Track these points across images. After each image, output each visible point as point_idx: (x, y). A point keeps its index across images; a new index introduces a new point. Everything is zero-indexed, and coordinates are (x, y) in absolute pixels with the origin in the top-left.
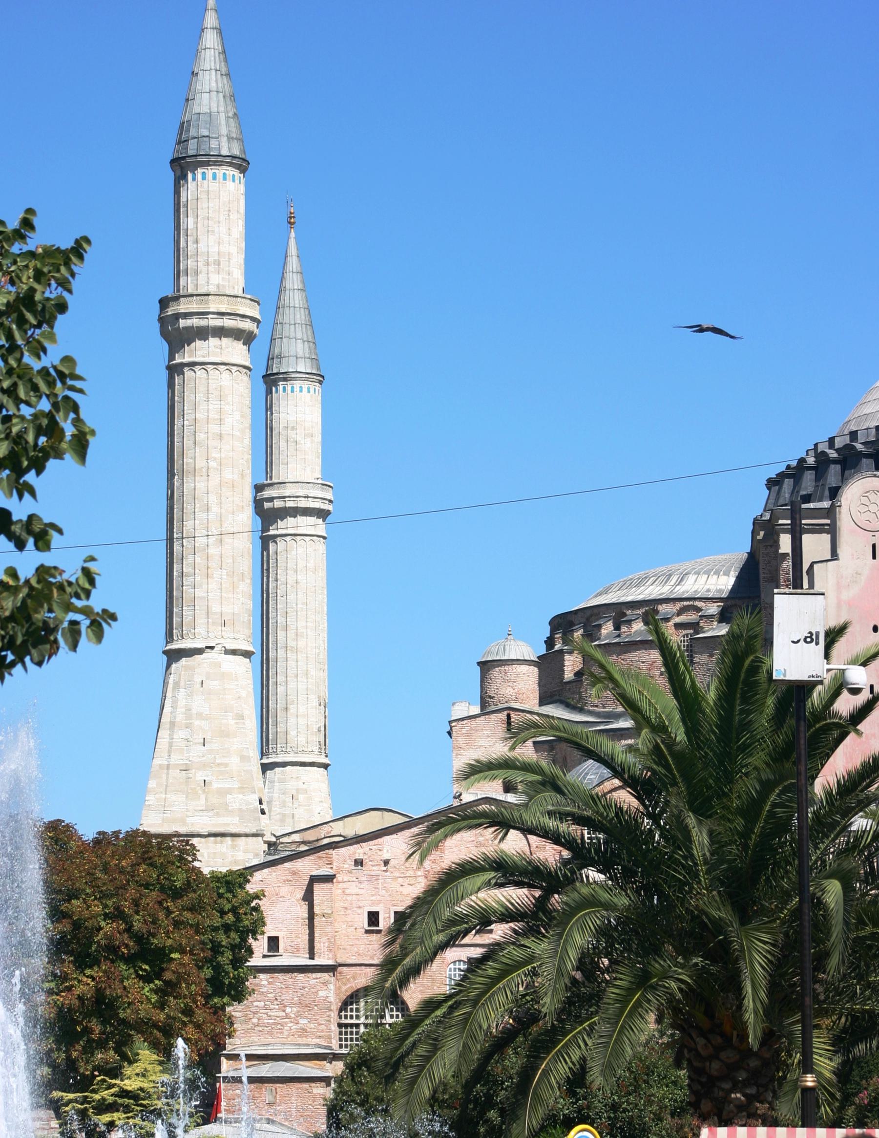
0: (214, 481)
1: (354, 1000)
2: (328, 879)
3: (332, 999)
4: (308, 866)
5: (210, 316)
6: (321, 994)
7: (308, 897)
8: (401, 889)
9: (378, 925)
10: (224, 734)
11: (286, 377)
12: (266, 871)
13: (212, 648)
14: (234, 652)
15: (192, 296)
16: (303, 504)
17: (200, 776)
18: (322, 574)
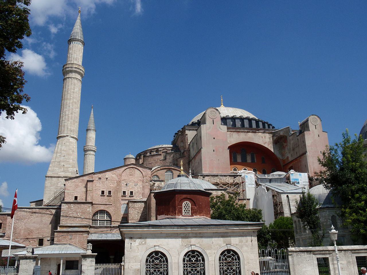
0: (71, 101)
1: (97, 214)
2: (92, 181)
3: (91, 211)
4: (86, 178)
5: (73, 68)
6: (88, 210)
7: (86, 187)
8: (110, 185)
9: (104, 194)
10: (69, 154)
11: (90, 130)
12: (75, 179)
13: (68, 136)
14: (73, 137)
15: (70, 64)
16: (91, 149)
17: (62, 164)
18: (94, 161)
